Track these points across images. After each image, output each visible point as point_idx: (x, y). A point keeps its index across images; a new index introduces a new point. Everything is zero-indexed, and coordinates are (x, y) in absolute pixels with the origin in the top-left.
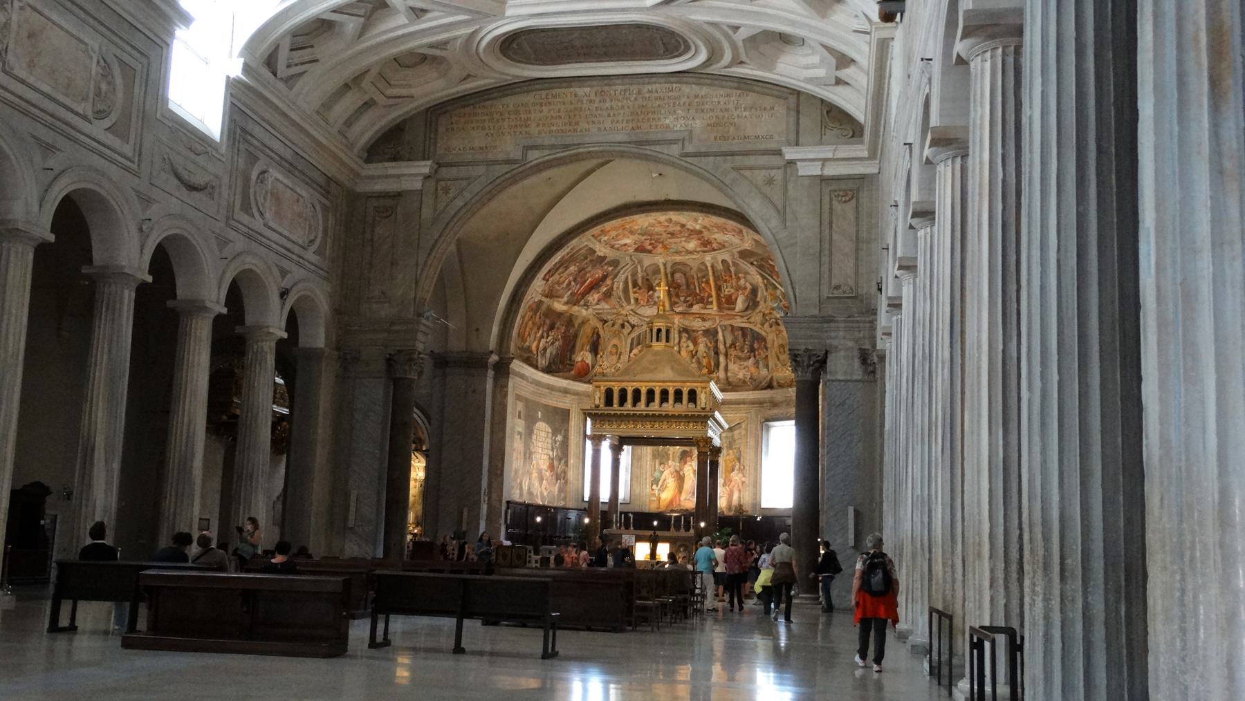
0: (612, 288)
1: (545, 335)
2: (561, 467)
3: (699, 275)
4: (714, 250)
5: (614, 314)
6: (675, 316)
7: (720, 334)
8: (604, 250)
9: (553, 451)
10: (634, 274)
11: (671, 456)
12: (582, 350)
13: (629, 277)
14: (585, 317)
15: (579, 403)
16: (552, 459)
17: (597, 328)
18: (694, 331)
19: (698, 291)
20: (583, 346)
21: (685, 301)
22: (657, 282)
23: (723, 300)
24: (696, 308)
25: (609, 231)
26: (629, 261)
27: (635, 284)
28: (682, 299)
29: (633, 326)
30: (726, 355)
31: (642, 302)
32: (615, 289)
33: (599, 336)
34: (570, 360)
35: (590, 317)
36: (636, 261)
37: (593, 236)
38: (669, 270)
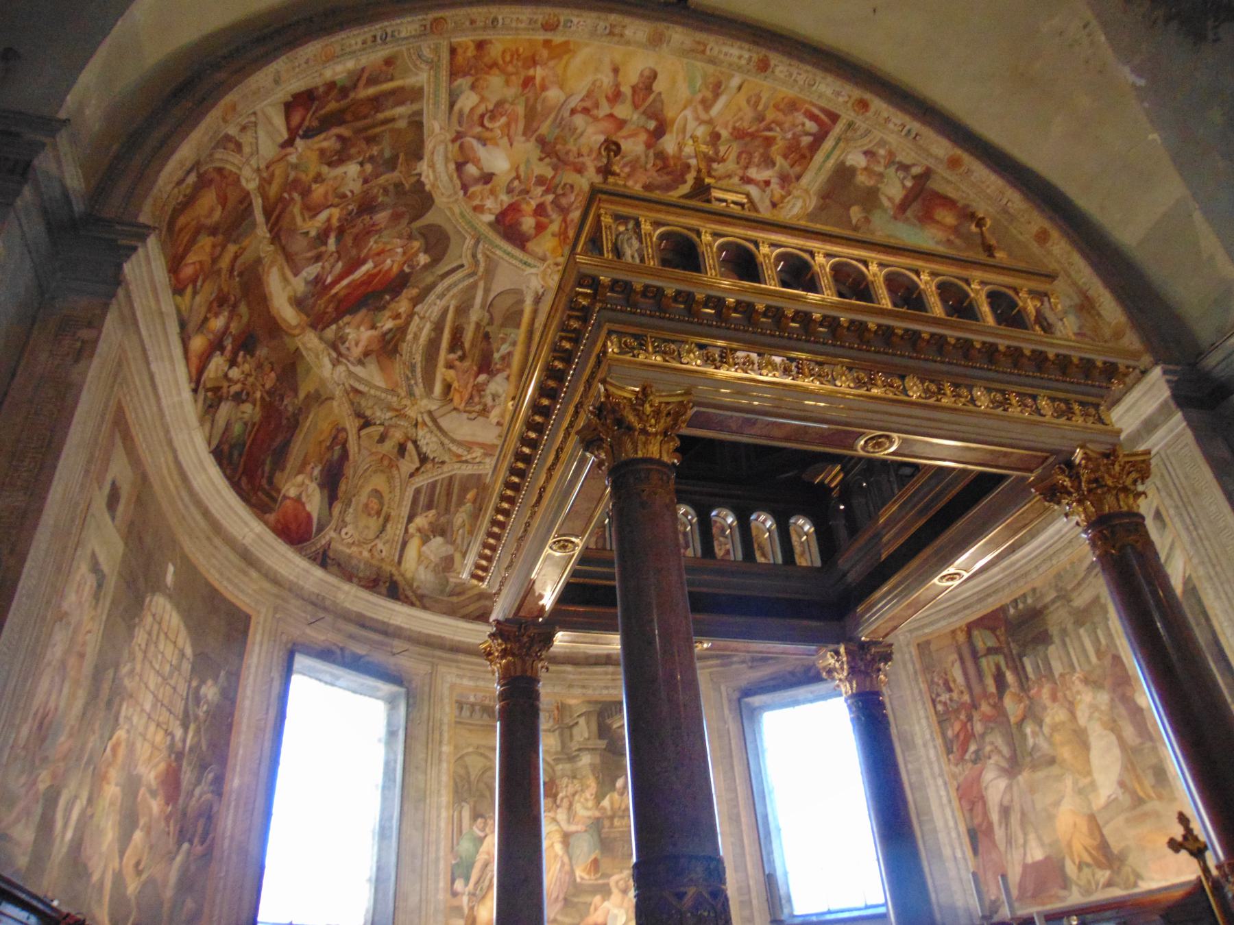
0: (402, 330)
1: (229, 347)
2: (202, 792)
5: (390, 408)
8: (440, 166)
9: (186, 727)
12: (299, 472)
14: (323, 382)
15: (276, 610)
16: (180, 756)
17: (344, 429)
20: (304, 463)
22: (505, 349)
25: (494, 65)
26: (466, 260)
29: (423, 459)
32: (409, 337)
33: (345, 455)
34: (270, 481)
35: (338, 392)
36: (481, 269)
37: (453, 51)
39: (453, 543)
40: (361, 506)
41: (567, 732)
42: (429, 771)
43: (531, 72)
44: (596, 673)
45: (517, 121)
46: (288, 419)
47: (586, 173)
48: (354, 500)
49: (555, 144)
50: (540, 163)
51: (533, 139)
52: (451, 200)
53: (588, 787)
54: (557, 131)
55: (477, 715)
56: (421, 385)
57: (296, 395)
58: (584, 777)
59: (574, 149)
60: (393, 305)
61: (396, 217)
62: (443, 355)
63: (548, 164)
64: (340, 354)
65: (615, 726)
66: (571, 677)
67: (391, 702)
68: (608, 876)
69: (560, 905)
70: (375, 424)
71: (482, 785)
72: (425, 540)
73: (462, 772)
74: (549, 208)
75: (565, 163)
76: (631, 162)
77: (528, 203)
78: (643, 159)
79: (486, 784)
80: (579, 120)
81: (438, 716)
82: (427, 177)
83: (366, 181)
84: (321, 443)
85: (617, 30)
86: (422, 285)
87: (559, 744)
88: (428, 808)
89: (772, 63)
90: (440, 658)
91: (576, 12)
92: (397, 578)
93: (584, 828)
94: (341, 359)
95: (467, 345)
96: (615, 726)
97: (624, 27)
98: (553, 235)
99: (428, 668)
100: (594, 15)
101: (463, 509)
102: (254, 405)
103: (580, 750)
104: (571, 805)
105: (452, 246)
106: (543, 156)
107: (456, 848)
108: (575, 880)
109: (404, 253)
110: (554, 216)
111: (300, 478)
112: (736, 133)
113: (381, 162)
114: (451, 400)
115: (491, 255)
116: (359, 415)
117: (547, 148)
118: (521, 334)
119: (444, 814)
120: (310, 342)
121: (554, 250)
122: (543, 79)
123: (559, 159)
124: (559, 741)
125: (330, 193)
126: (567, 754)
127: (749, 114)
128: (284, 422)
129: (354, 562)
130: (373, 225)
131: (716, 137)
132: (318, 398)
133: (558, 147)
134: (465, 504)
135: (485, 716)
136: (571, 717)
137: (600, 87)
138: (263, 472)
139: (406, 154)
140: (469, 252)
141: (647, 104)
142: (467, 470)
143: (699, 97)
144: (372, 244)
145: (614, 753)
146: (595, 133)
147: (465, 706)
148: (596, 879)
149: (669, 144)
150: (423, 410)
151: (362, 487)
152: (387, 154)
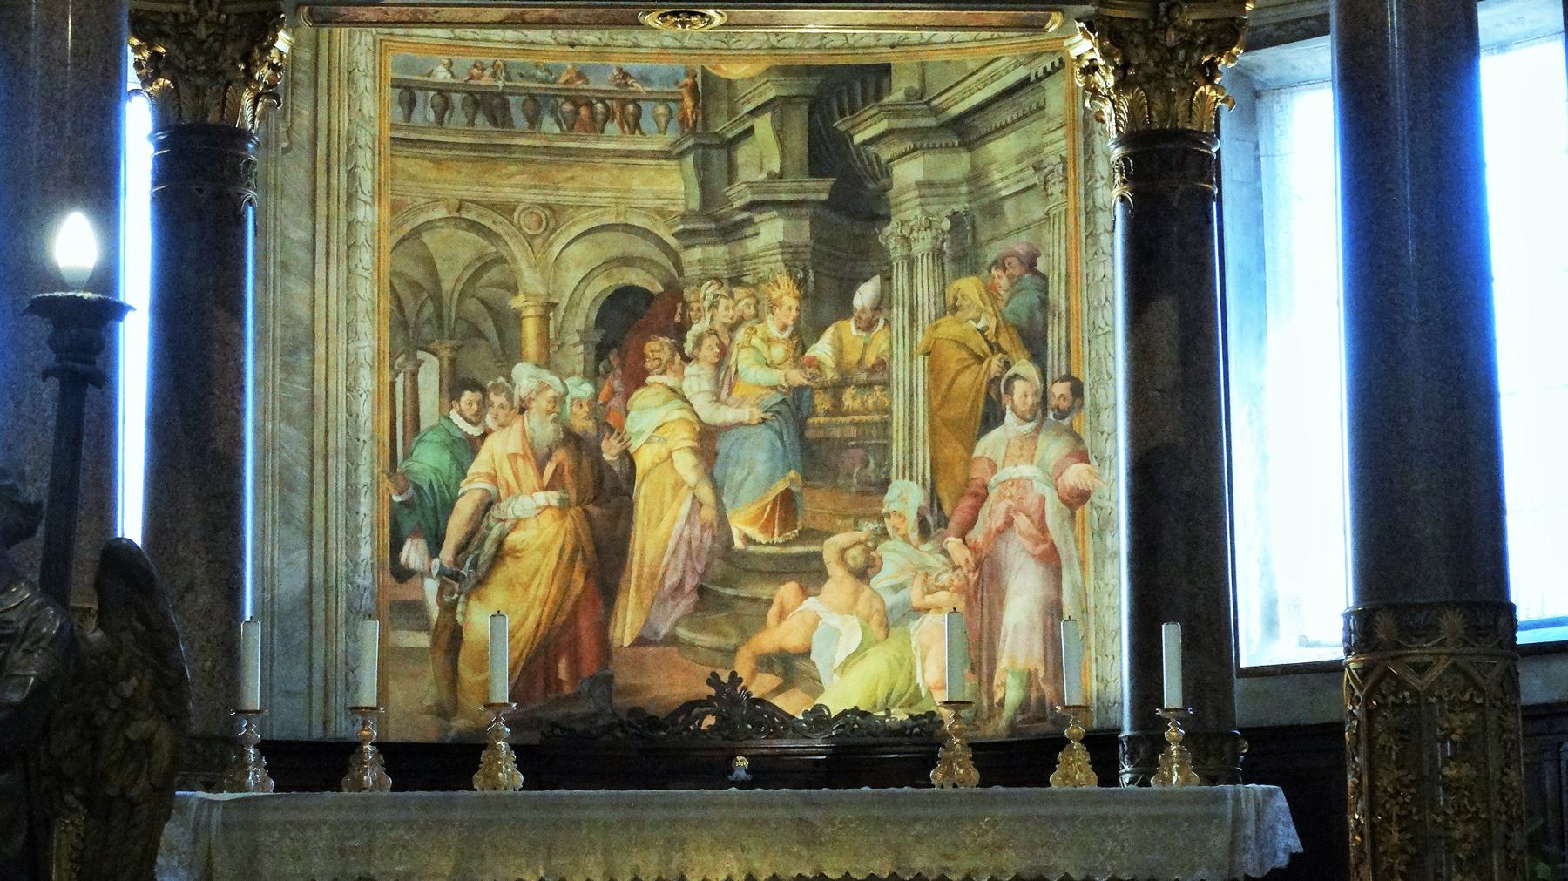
11: (530, 328)
41: (718, 158)
42: (320, 273)
53: (773, 305)
55: (459, 117)
58: (762, 280)
65: (858, 139)
68: (821, 535)
69: (685, 604)
71: (472, 306)
73: (418, 273)
79: (483, 302)
81: (342, 122)
87: (696, 192)
88: (320, 369)
93: (758, 414)
96: (858, 139)
103: (752, 206)
104: (724, 352)
107: (401, 468)
108: (730, 540)
119: (366, 380)
124: (694, 180)
126: (717, 220)
135: (481, 120)
136: (732, 112)
145: (854, 215)
147: (420, 95)
148: (787, 543)
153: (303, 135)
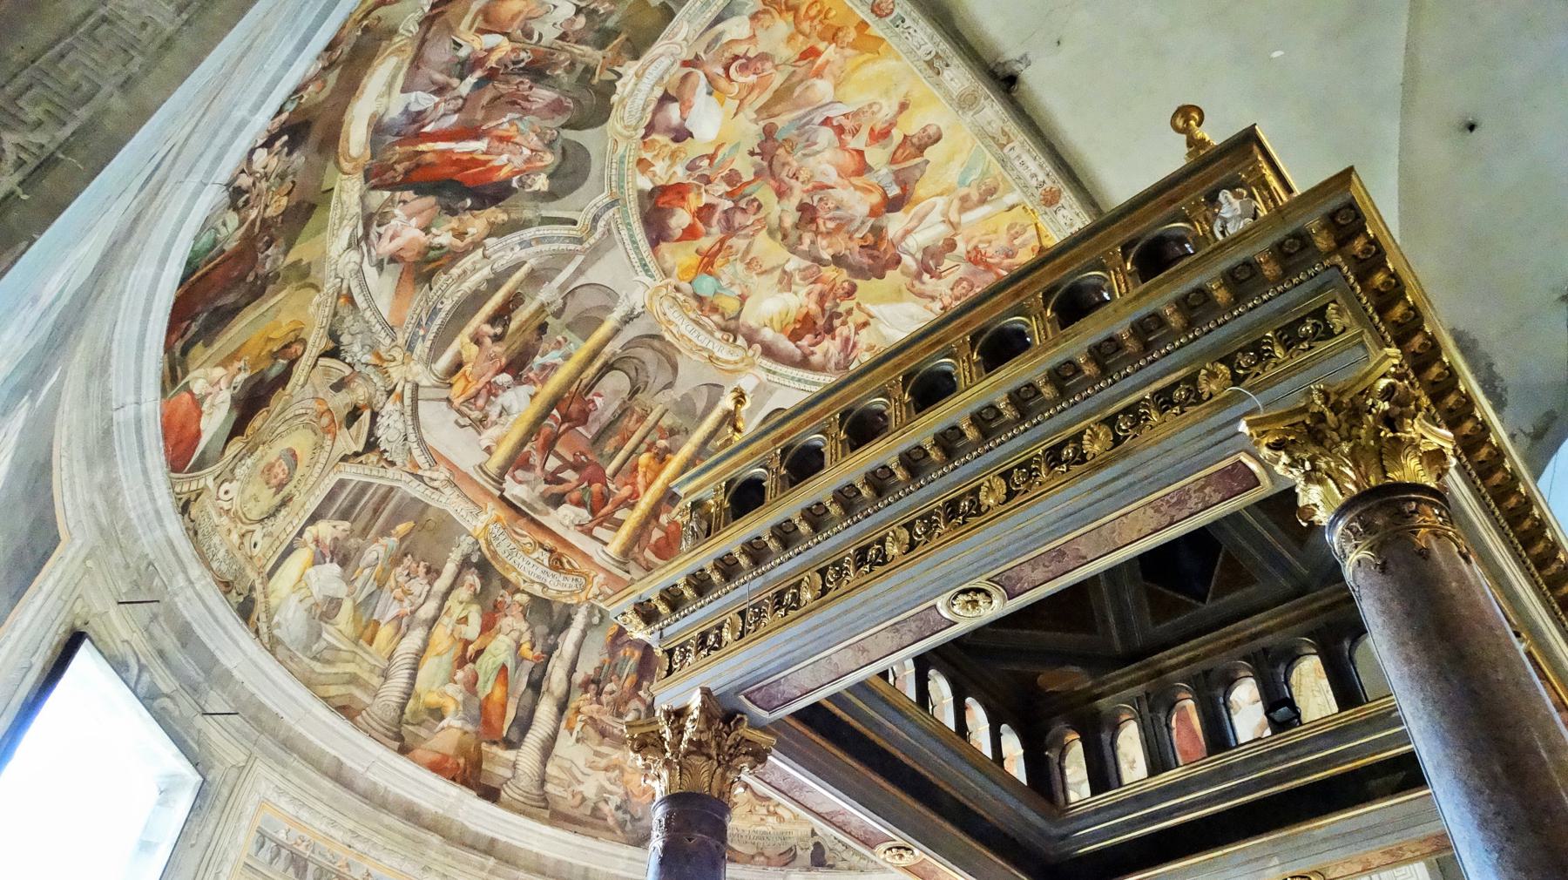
0: (455, 256)
3: (666, 422)
4: (804, 363)
5: (374, 349)
6: (491, 505)
7: (573, 633)
10: (536, 278)
13: (525, 269)
17: (304, 342)
18: (505, 583)
19: (609, 470)
21: (553, 479)
22: (553, 357)
23: (657, 534)
24: (564, 518)
26: (583, 219)
27: (501, 316)
28: (553, 463)
29: (371, 445)
30: (562, 707)
31: (459, 385)
32: (455, 271)
33: (284, 378)
35: (329, 286)
36: (592, 241)
38: (615, 347)
39: (350, 582)
40: (262, 464)
43: (821, 46)
44: (468, 862)
45: (760, 94)
46: (256, 276)
47: (785, 202)
48: (261, 448)
49: (781, 146)
50: (750, 158)
51: (762, 124)
52: (626, 133)
54: (796, 132)
55: (280, 864)
56: (428, 344)
57: (286, 253)
59: (795, 164)
60: (467, 216)
61: (556, 108)
62: (478, 321)
63: (754, 165)
64: (366, 236)
66: (433, 854)
67: (166, 793)
70: (343, 361)
72: (318, 560)
74: (717, 216)
75: (773, 175)
76: (840, 219)
77: (699, 195)
78: (857, 224)
80: (826, 135)
81: (225, 842)
82: (625, 85)
83: (563, 37)
84: (269, 339)
85: (937, 64)
86: (514, 216)
89: (1062, 201)
90: (264, 750)
91: (916, 14)
92: (258, 595)
94: (363, 244)
95: (513, 325)
97: (947, 65)
98: (697, 251)
99: (241, 758)
100: (930, 30)
101: (385, 541)
102: (242, 223)
105: (581, 189)
106: (757, 150)
109: (528, 160)
110: (716, 231)
111: (219, 372)
112: (973, 255)
113: (597, 27)
114: (451, 385)
115: (615, 231)
116: (334, 335)
117: (769, 147)
118: (582, 350)
120: (349, 192)
121: (685, 271)
122: (828, 62)
123: (770, 165)
125: (521, 17)
127: (1002, 241)
128: (250, 278)
129: (216, 540)
130: (526, 99)
131: (951, 245)
132: (303, 276)
133: (781, 151)
134: (390, 535)
135: (291, 870)
137: (873, 113)
138: (187, 329)
139: (628, 39)
140: (594, 210)
141: (907, 164)
142: (416, 490)
143: (963, 191)
144: (505, 122)
146: (828, 162)
147: (268, 844)
149: (895, 224)
150: (410, 378)
151: (280, 435)
152: (610, 23)
153: (204, 841)
